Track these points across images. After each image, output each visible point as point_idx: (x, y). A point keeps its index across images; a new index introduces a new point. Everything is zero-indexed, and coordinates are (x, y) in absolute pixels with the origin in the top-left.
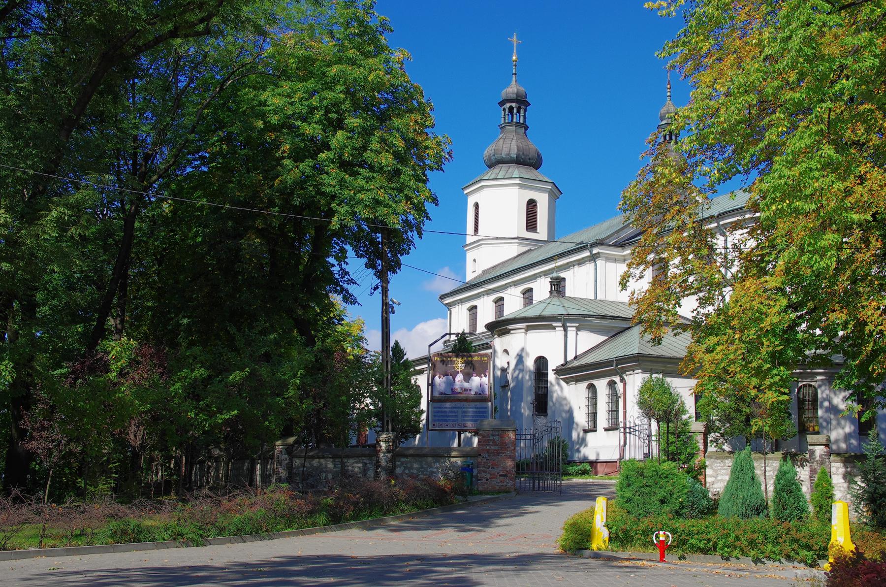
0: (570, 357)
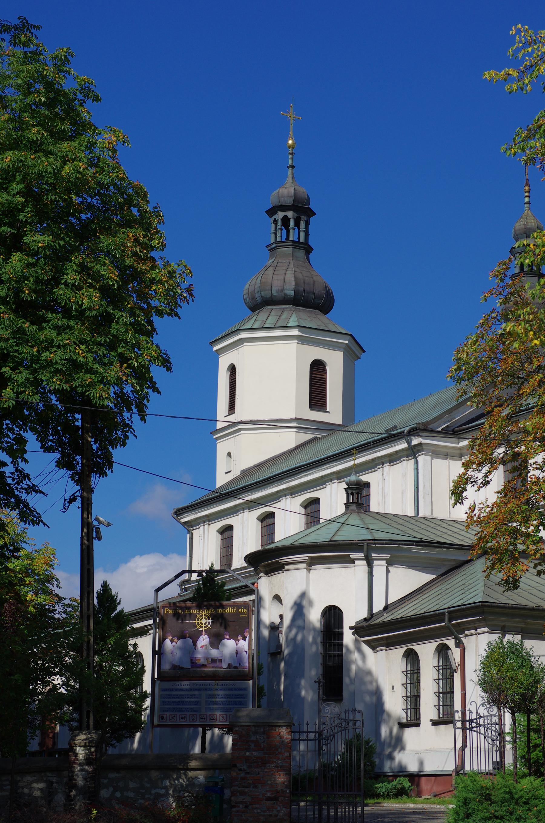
0: (378, 606)
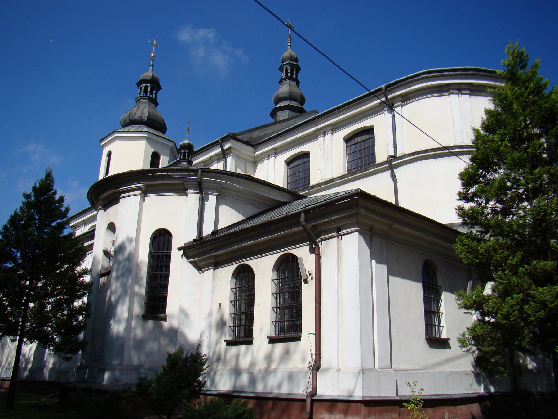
0: (208, 230)
